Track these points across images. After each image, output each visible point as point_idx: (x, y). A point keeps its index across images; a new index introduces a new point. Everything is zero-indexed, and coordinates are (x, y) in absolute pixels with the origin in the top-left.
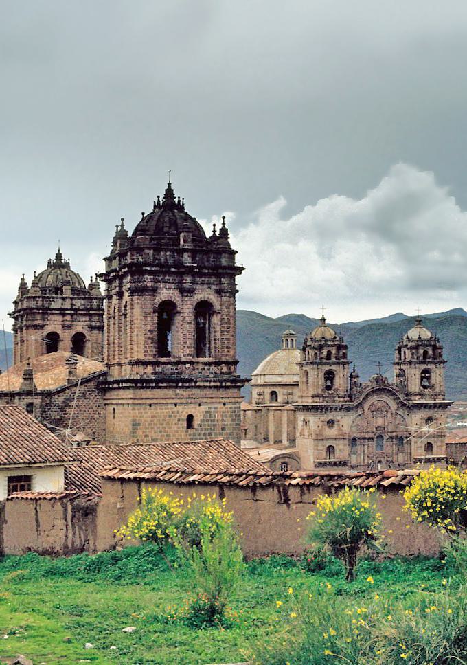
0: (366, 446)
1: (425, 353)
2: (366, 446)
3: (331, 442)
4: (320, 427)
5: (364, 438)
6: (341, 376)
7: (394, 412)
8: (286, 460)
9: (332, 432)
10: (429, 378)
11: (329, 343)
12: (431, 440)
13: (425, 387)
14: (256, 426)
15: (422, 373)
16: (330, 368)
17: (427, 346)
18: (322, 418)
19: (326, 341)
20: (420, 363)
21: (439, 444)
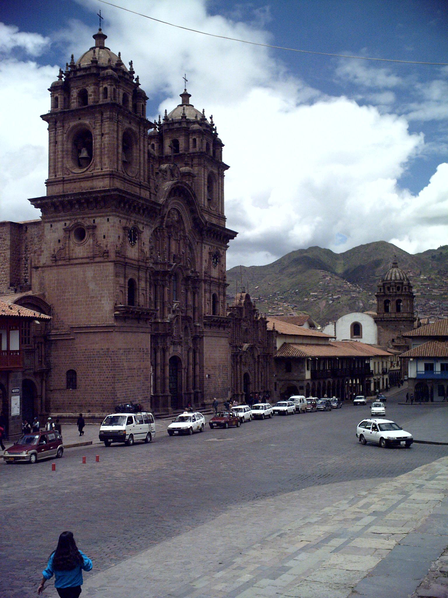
4: (121, 240)
5: (165, 273)
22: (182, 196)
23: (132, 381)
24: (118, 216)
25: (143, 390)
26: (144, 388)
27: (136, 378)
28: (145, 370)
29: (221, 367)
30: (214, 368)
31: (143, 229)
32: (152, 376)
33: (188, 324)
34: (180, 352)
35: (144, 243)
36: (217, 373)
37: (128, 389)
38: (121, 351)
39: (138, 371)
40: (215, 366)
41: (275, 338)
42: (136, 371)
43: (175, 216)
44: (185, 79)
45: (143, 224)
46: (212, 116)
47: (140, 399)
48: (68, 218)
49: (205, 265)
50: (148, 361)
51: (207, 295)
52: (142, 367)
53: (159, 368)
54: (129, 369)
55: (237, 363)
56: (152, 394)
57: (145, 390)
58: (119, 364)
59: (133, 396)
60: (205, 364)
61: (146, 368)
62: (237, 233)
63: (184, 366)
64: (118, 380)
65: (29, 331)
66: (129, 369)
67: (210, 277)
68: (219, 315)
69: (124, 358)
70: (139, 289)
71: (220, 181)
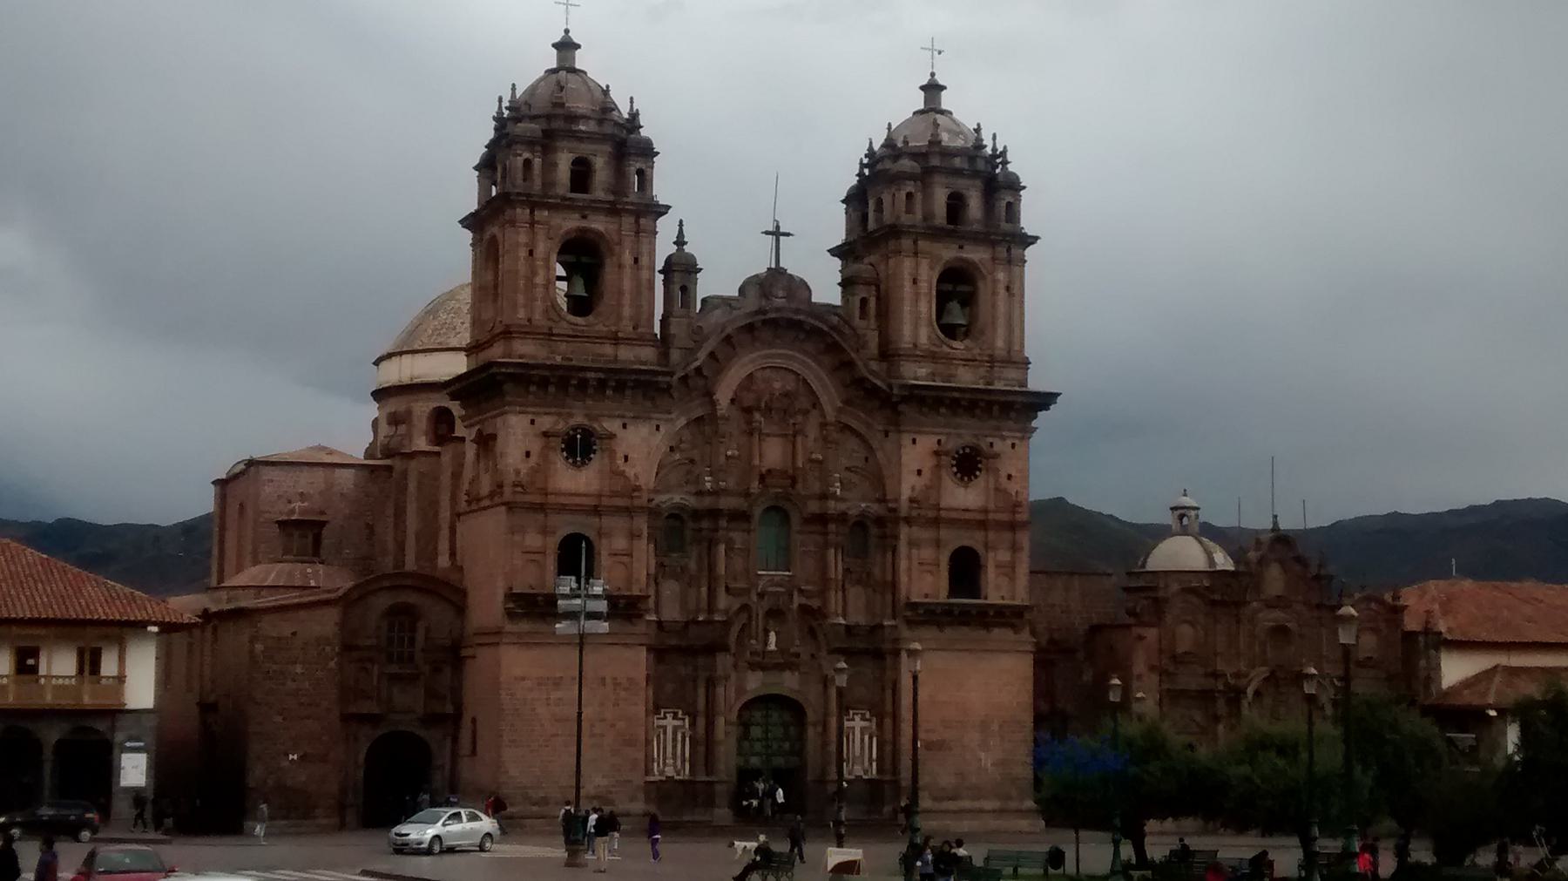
0: (722, 548)
1: (956, 204)
2: (722, 548)
3: (581, 518)
4: (534, 459)
5: (714, 514)
6: (627, 258)
7: (831, 416)
8: (412, 598)
9: (574, 481)
10: (968, 301)
11: (582, 128)
12: (973, 539)
13: (950, 331)
14: (370, 527)
15: (942, 279)
16: (584, 224)
17: (958, 172)
18: (546, 422)
19: (573, 118)
20: (936, 234)
21: (1004, 556)
22: (802, 336)
24: (520, 413)
29: (995, 727)
31: (624, 426)
32: (687, 739)
33: (815, 624)
34: (796, 687)
35: (626, 458)
38: (528, 683)
41: (1433, 652)
43: (777, 385)
44: (932, 50)
45: (618, 416)
46: (979, 125)
48: (477, 419)
49: (908, 486)
50: (636, 704)
51: (927, 553)
53: (701, 722)
54: (556, 720)
55: (1216, 719)
56: (686, 778)
62: (1059, 394)
63: (811, 716)
64: (510, 741)
65: (412, 641)
67: (940, 509)
68: (986, 598)
70: (600, 554)
71: (1001, 276)
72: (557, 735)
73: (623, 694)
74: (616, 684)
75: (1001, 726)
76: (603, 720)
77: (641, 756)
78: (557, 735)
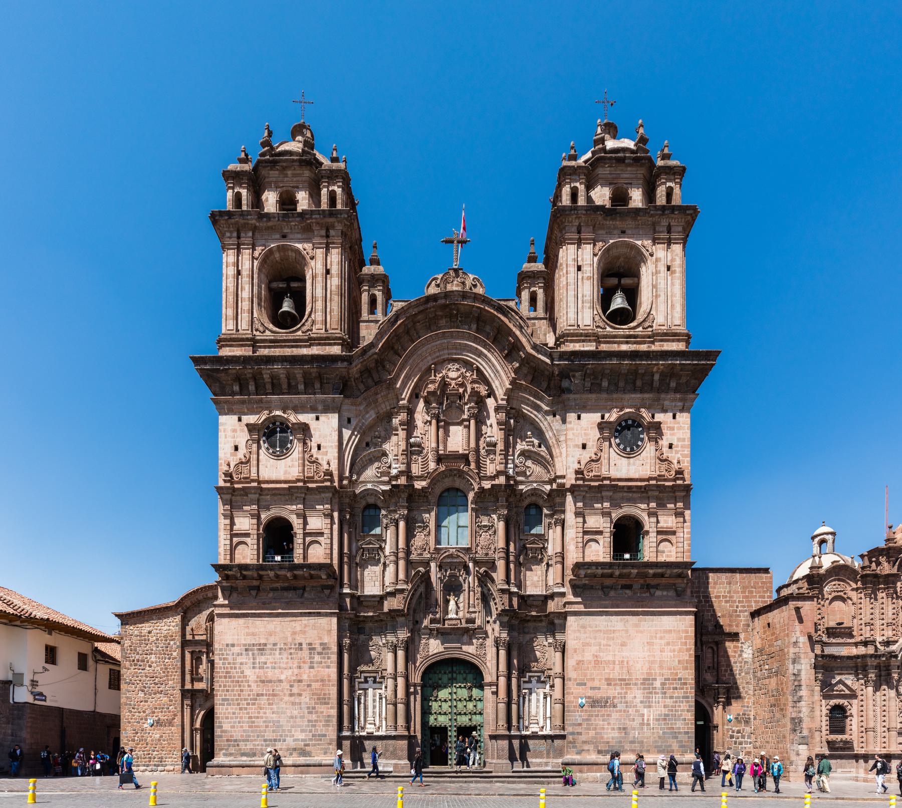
23: (269, 704)
25: (309, 721)
26: (314, 717)
27: (287, 698)
28: (315, 685)
29: (657, 684)
30: (625, 683)
36: (636, 695)
37: (258, 717)
39: (291, 686)
40: (624, 680)
42: (285, 685)
47: (300, 737)
50: (328, 667)
52: (305, 677)
54: (263, 682)
57: (316, 721)
58: (227, 673)
59: (274, 731)
60: (570, 673)
61: (322, 681)
64: (223, 700)
66: (263, 682)
69: (244, 661)
72: (262, 695)
73: (317, 658)
74: (312, 649)
75: (663, 684)
76: (300, 681)
77: (334, 712)
78: (262, 695)
